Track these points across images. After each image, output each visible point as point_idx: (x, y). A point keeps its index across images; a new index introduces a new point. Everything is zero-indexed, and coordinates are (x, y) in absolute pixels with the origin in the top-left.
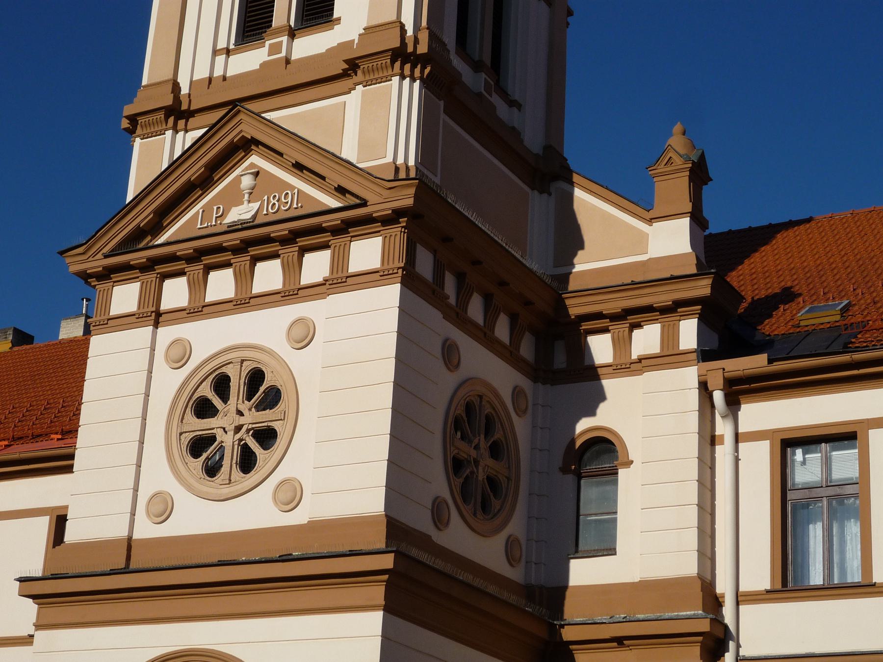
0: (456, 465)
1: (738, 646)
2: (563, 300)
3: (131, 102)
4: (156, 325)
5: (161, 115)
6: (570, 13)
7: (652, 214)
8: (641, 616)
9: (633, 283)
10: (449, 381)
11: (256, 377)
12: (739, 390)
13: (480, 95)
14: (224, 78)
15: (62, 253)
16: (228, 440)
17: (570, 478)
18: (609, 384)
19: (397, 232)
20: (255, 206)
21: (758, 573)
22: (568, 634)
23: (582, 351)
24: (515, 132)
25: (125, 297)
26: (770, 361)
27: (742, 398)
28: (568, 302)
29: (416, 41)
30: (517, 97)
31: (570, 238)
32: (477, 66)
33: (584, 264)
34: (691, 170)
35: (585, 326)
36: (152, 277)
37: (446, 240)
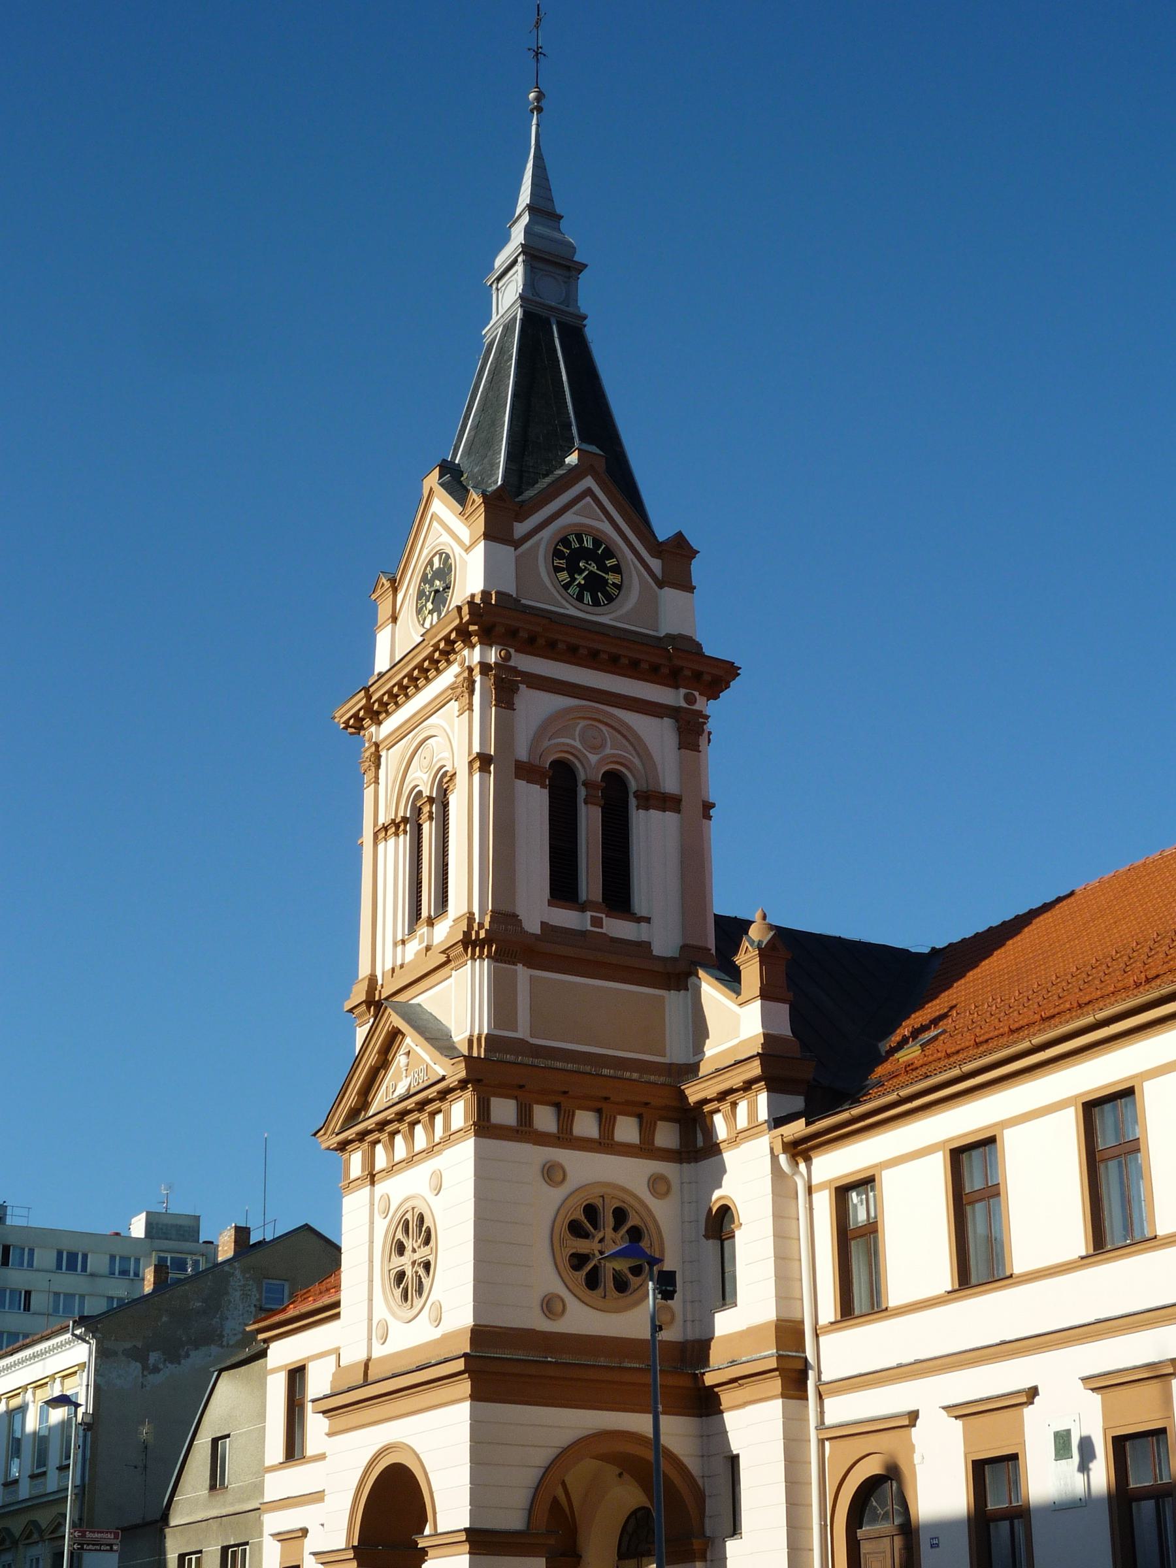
0: (578, 1261)
1: (819, 1373)
2: (683, 1091)
3: (348, 998)
4: (373, 1183)
5: (364, 1007)
6: (713, 806)
7: (741, 999)
8: (744, 1359)
9: (717, 1070)
10: (557, 1195)
11: (421, 1219)
12: (800, 1150)
13: (583, 934)
14: (402, 966)
15: (315, 1134)
16: (409, 1272)
17: (711, 1245)
18: (730, 1157)
19: (468, 1094)
20: (409, 1079)
21: (828, 1310)
22: (710, 1379)
23: (709, 1131)
24: (646, 946)
25: (356, 1161)
26: (807, 1124)
27: (812, 1154)
28: (687, 1092)
29: (481, 925)
30: (644, 913)
31: (699, 1031)
32: (583, 908)
33: (712, 1049)
34: (760, 955)
35: (707, 1108)
36: (365, 1145)
37: (521, 1087)
